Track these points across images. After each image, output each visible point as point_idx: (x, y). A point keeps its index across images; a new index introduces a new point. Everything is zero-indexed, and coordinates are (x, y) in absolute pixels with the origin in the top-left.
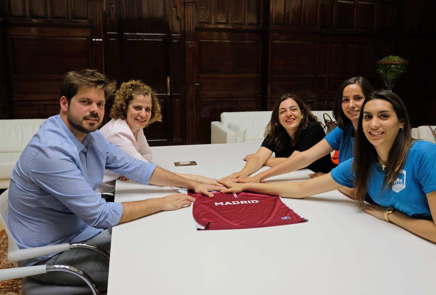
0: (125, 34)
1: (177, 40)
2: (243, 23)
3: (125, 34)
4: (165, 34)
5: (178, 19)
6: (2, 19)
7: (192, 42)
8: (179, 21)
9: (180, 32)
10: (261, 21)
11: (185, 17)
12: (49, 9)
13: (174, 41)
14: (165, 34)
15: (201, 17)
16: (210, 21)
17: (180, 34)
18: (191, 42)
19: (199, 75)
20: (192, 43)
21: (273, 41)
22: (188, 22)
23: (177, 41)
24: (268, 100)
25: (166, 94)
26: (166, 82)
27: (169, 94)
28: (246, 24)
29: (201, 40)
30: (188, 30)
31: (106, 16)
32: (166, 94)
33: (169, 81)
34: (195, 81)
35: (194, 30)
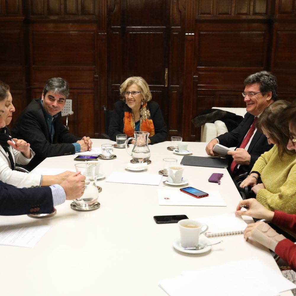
0: (127, 28)
2: (248, 13)
3: (127, 27)
4: (165, 27)
6: (24, 18)
12: (63, 6)
13: (175, 33)
16: (212, 12)
18: (190, 34)
20: (191, 35)
21: (278, 32)
23: (177, 33)
27: (166, 86)
29: (202, 33)
31: (110, 11)
33: (166, 73)
34: (193, 74)
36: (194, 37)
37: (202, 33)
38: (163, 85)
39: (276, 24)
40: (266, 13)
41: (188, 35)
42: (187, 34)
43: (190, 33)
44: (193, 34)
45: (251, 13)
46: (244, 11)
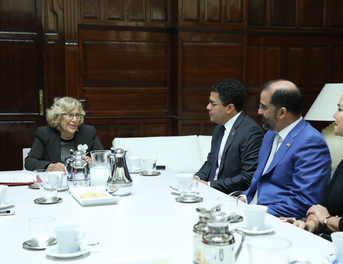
1: (53, 40)
2: (144, 19)
4: (36, 34)
5: (55, 13)
7: (74, 44)
8: (55, 15)
9: (57, 31)
10: (169, 17)
11: (63, 10)
13: (50, 42)
14: (36, 34)
15: (86, 11)
16: (98, 16)
17: (57, 33)
18: (72, 44)
19: (84, 88)
20: (73, 45)
21: (183, 43)
22: (67, 17)
23: (53, 42)
24: (180, 122)
25: (38, 114)
26: (38, 97)
27: (41, 114)
28: (148, 20)
30: (68, 28)
32: (38, 114)
33: (41, 96)
35: (77, 27)
36: (77, 48)
37: (86, 42)
38: (36, 112)
39: (181, 34)
40: (165, 21)
41: (69, 45)
42: (66, 44)
43: (71, 42)
44: (77, 44)
45: (148, 20)
46: (140, 17)
